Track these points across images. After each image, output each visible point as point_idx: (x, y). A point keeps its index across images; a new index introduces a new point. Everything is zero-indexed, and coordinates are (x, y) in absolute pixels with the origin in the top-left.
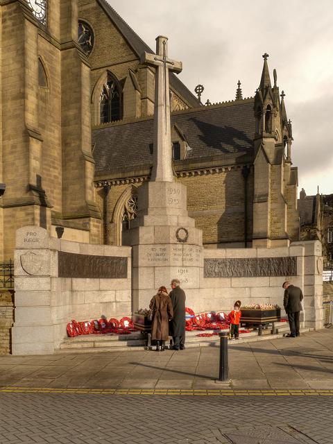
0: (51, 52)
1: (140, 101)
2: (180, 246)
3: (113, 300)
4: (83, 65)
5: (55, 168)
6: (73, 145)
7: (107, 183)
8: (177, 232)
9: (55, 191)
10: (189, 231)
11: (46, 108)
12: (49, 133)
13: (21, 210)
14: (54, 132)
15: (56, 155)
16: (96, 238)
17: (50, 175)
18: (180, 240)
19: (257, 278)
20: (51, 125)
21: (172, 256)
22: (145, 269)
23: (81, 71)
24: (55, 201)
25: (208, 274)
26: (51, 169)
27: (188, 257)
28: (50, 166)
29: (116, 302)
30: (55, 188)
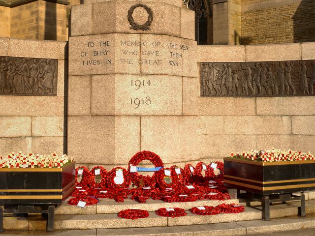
2: (134, 37)
3: (25, 133)
10: (154, 10)
13: (27, 8)
18: (135, 27)
19: (304, 99)
21: (118, 55)
22: (78, 78)
25: (206, 92)
27: (152, 58)
29: (32, 136)
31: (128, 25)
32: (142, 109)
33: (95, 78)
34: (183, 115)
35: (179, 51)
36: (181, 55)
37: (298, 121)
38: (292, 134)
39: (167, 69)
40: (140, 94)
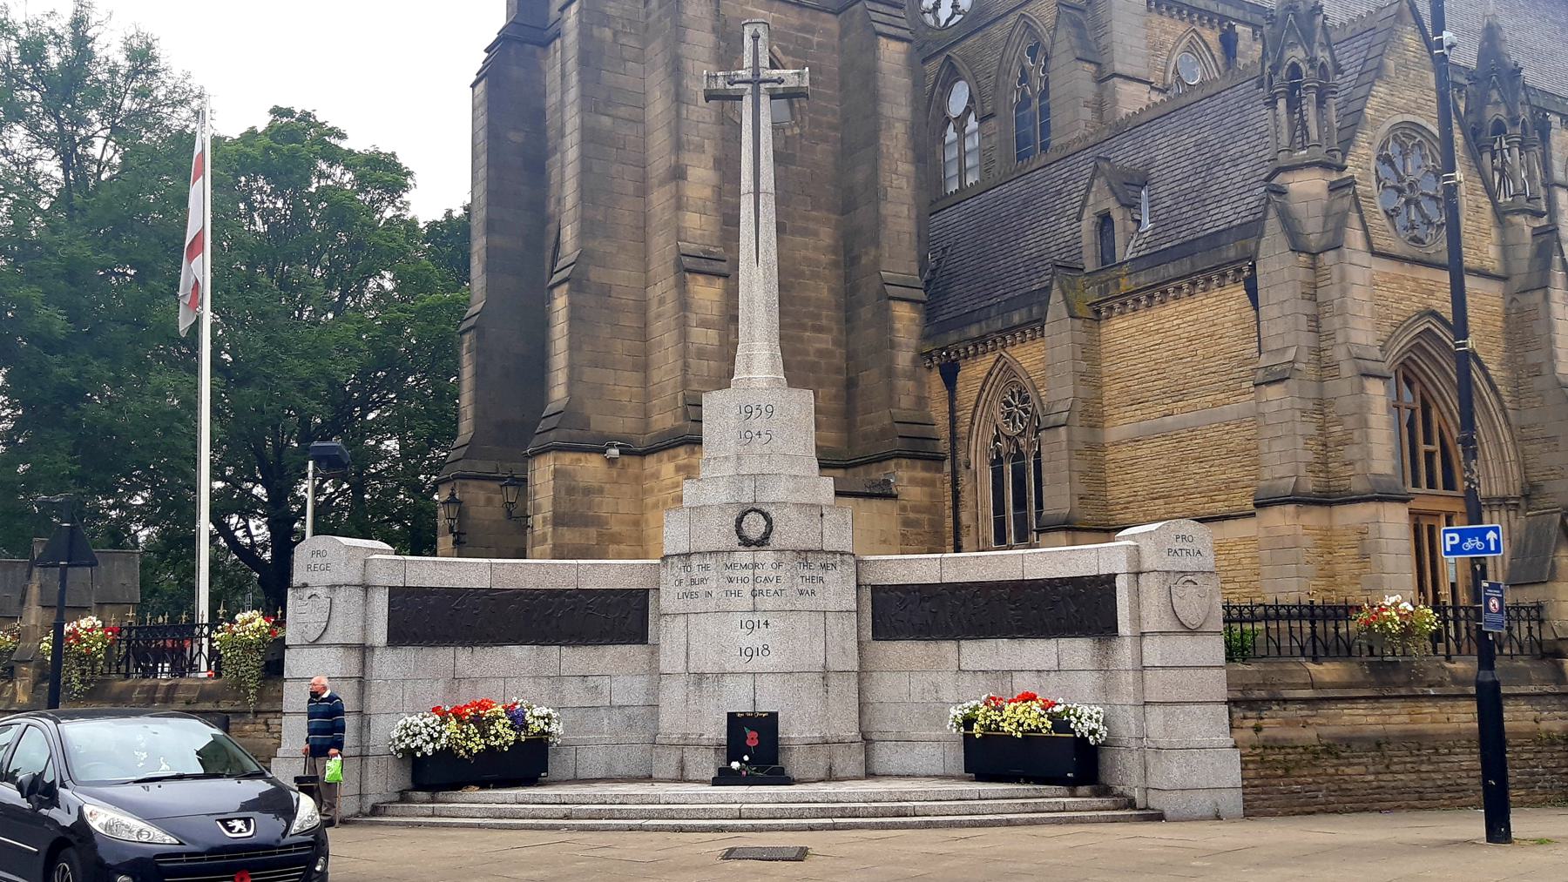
0: (803, 28)
1: (1092, 86)
2: (745, 557)
4: (883, 41)
5: (819, 329)
6: (864, 261)
10: (773, 515)
12: (798, 239)
14: (816, 234)
15: (824, 293)
16: (925, 517)
18: (746, 542)
23: (876, 59)
27: (771, 587)
28: (803, 327)
36: (821, 579)
40: (754, 640)
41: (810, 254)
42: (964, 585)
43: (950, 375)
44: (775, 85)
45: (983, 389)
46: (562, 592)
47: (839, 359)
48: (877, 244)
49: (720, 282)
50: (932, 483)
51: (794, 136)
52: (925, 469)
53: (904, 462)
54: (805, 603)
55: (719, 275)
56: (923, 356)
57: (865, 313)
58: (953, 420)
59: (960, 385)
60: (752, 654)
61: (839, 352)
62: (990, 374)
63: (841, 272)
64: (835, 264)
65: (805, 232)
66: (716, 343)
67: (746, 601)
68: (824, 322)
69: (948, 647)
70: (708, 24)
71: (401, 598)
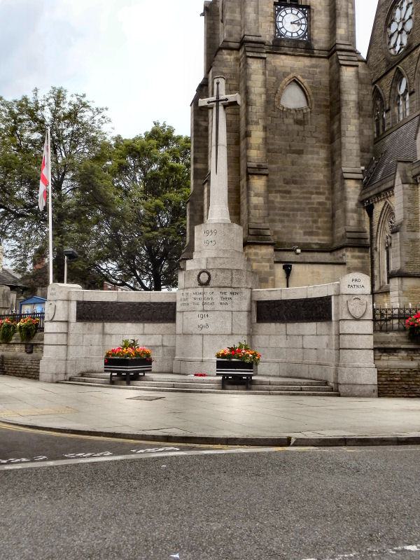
0: (312, 66)
2: (200, 290)
3: (159, 344)
7: (369, 202)
8: (199, 276)
9: (320, 220)
11: (304, 130)
12: (310, 156)
14: (318, 153)
17: (313, 203)
18: (201, 284)
20: (312, 147)
23: (339, 76)
24: (320, 231)
26: (313, 196)
27: (210, 301)
30: (319, 217)
31: (197, 283)
32: (204, 331)
33: (184, 313)
34: (232, 334)
35: (228, 295)
37: (306, 338)
38: (303, 348)
39: (220, 307)
40: (203, 322)
41: (315, 162)
42: (289, 301)
43: (370, 210)
44: (225, 102)
45: (381, 216)
46: (145, 303)
47: (329, 205)
48: (340, 155)
49: (265, 177)
50: (363, 258)
51: (307, 113)
52: (359, 252)
53: (349, 249)
54: (224, 307)
55: (264, 175)
56: (361, 202)
57: (337, 185)
58: (371, 230)
59: (374, 215)
60: (201, 327)
61: (329, 203)
62: (383, 209)
63: (330, 168)
64: (327, 165)
65: (312, 153)
66: (263, 202)
67: (200, 307)
68: (321, 190)
69: (282, 326)
70: (261, 71)
71: (81, 305)
